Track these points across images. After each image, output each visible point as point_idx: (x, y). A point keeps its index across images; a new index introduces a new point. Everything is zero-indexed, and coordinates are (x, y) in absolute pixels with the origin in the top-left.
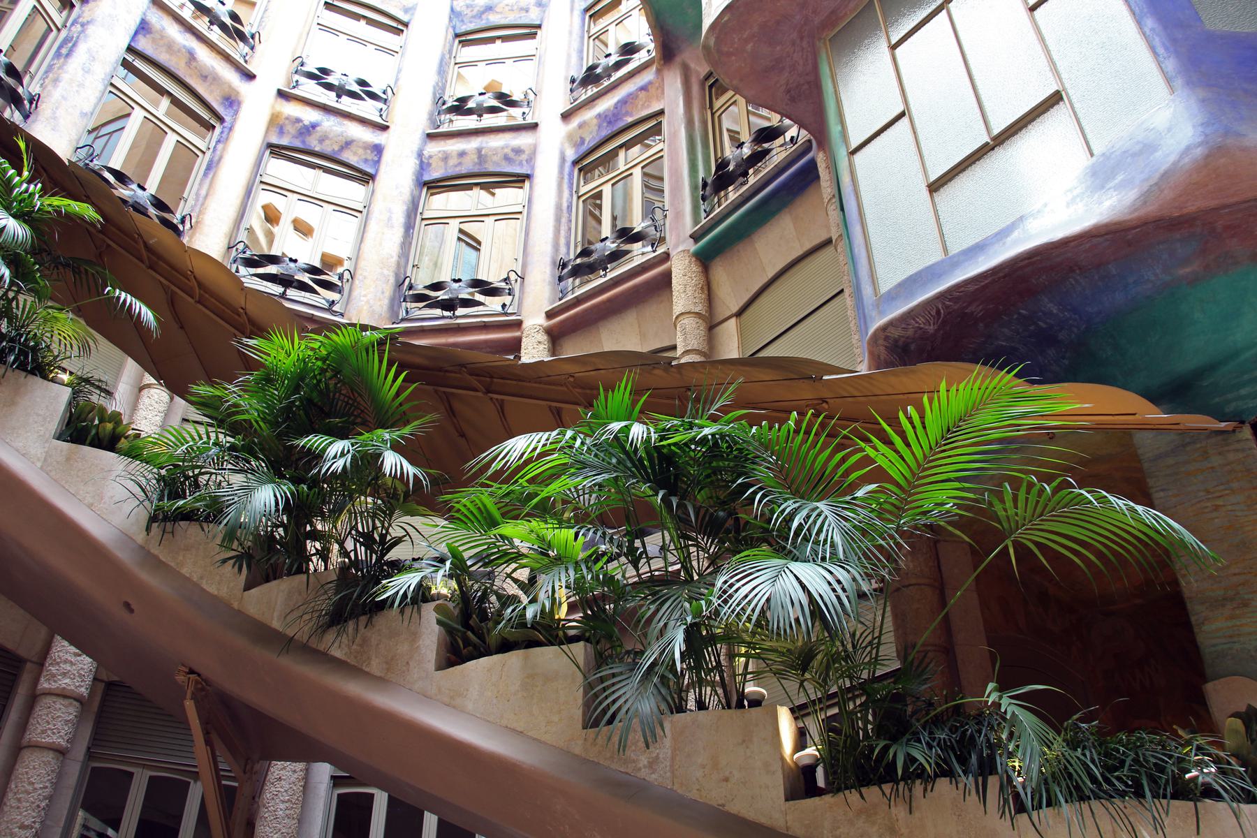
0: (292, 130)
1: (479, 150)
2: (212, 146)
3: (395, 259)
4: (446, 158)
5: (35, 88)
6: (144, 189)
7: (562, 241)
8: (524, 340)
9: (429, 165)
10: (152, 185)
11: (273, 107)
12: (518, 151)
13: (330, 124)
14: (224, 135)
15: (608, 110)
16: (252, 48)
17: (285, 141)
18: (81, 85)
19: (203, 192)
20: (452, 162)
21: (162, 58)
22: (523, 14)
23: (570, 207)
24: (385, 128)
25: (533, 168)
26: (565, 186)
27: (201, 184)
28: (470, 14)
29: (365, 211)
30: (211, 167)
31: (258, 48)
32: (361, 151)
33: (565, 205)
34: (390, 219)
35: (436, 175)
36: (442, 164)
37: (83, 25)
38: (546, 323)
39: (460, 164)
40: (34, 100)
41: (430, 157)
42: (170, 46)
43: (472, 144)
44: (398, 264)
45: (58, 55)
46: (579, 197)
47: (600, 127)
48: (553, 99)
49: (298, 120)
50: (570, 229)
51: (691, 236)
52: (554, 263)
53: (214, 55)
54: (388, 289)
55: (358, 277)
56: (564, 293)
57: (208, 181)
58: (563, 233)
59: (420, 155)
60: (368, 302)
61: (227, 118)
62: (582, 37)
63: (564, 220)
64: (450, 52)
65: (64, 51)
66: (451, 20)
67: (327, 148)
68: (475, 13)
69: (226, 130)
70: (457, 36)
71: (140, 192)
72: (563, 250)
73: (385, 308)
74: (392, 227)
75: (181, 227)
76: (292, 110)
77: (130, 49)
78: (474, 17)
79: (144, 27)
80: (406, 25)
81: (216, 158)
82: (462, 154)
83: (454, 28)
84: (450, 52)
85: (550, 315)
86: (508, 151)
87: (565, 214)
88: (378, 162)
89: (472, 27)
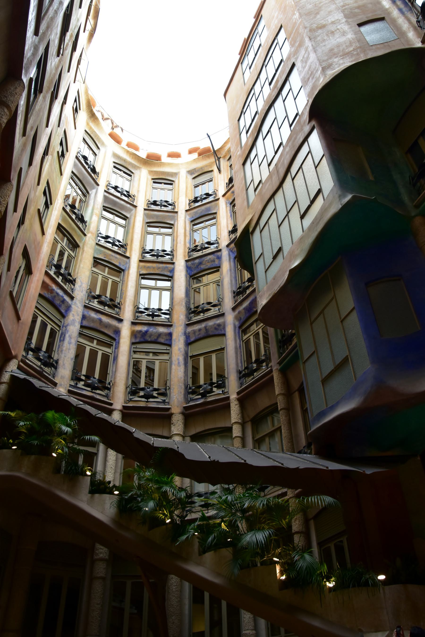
0: (139, 335)
1: (205, 327)
2: (113, 351)
3: (183, 379)
4: (194, 332)
5: (55, 358)
6: (95, 378)
7: (239, 361)
8: (231, 404)
9: (189, 336)
10: (97, 375)
11: (131, 329)
12: (219, 325)
13: (152, 330)
14: (117, 345)
15: (247, 306)
16: (120, 308)
17: (138, 340)
18: (69, 349)
19: (114, 370)
20: (197, 334)
21: (92, 325)
22: (213, 263)
23: (240, 346)
24: (171, 326)
25: (225, 331)
26: (237, 338)
27: (113, 367)
28: (194, 267)
29: (170, 360)
30: (116, 359)
31: (122, 307)
32: (164, 337)
33: (238, 346)
34: (179, 363)
35: (192, 339)
36: (194, 335)
37: (66, 327)
38: (237, 397)
39: (200, 334)
40: (57, 362)
41: (189, 333)
42: (93, 320)
43: (203, 325)
44: (185, 380)
45: (60, 341)
46: (243, 341)
47: (245, 313)
48: (228, 302)
49: (141, 331)
50: (241, 355)
51: (278, 363)
52: (237, 371)
53: (107, 317)
54: (183, 391)
55: (172, 388)
56: (241, 384)
57: (115, 365)
58: (239, 358)
59: (185, 333)
60: (176, 398)
61: (117, 338)
62: (235, 271)
63: (239, 353)
64: (189, 285)
65: (62, 339)
66: (187, 271)
67: (153, 338)
68: (195, 266)
69: (117, 343)
70: (191, 276)
71: (94, 380)
72: (240, 365)
73: (183, 398)
74: (180, 366)
75: (109, 386)
76: (138, 328)
77: (82, 327)
78: (195, 268)
79: (84, 317)
80: (172, 277)
81: (116, 355)
82: (200, 330)
83: (189, 274)
84: (189, 285)
85: (238, 393)
86: (215, 326)
87: (239, 350)
88: (171, 339)
89: (195, 272)
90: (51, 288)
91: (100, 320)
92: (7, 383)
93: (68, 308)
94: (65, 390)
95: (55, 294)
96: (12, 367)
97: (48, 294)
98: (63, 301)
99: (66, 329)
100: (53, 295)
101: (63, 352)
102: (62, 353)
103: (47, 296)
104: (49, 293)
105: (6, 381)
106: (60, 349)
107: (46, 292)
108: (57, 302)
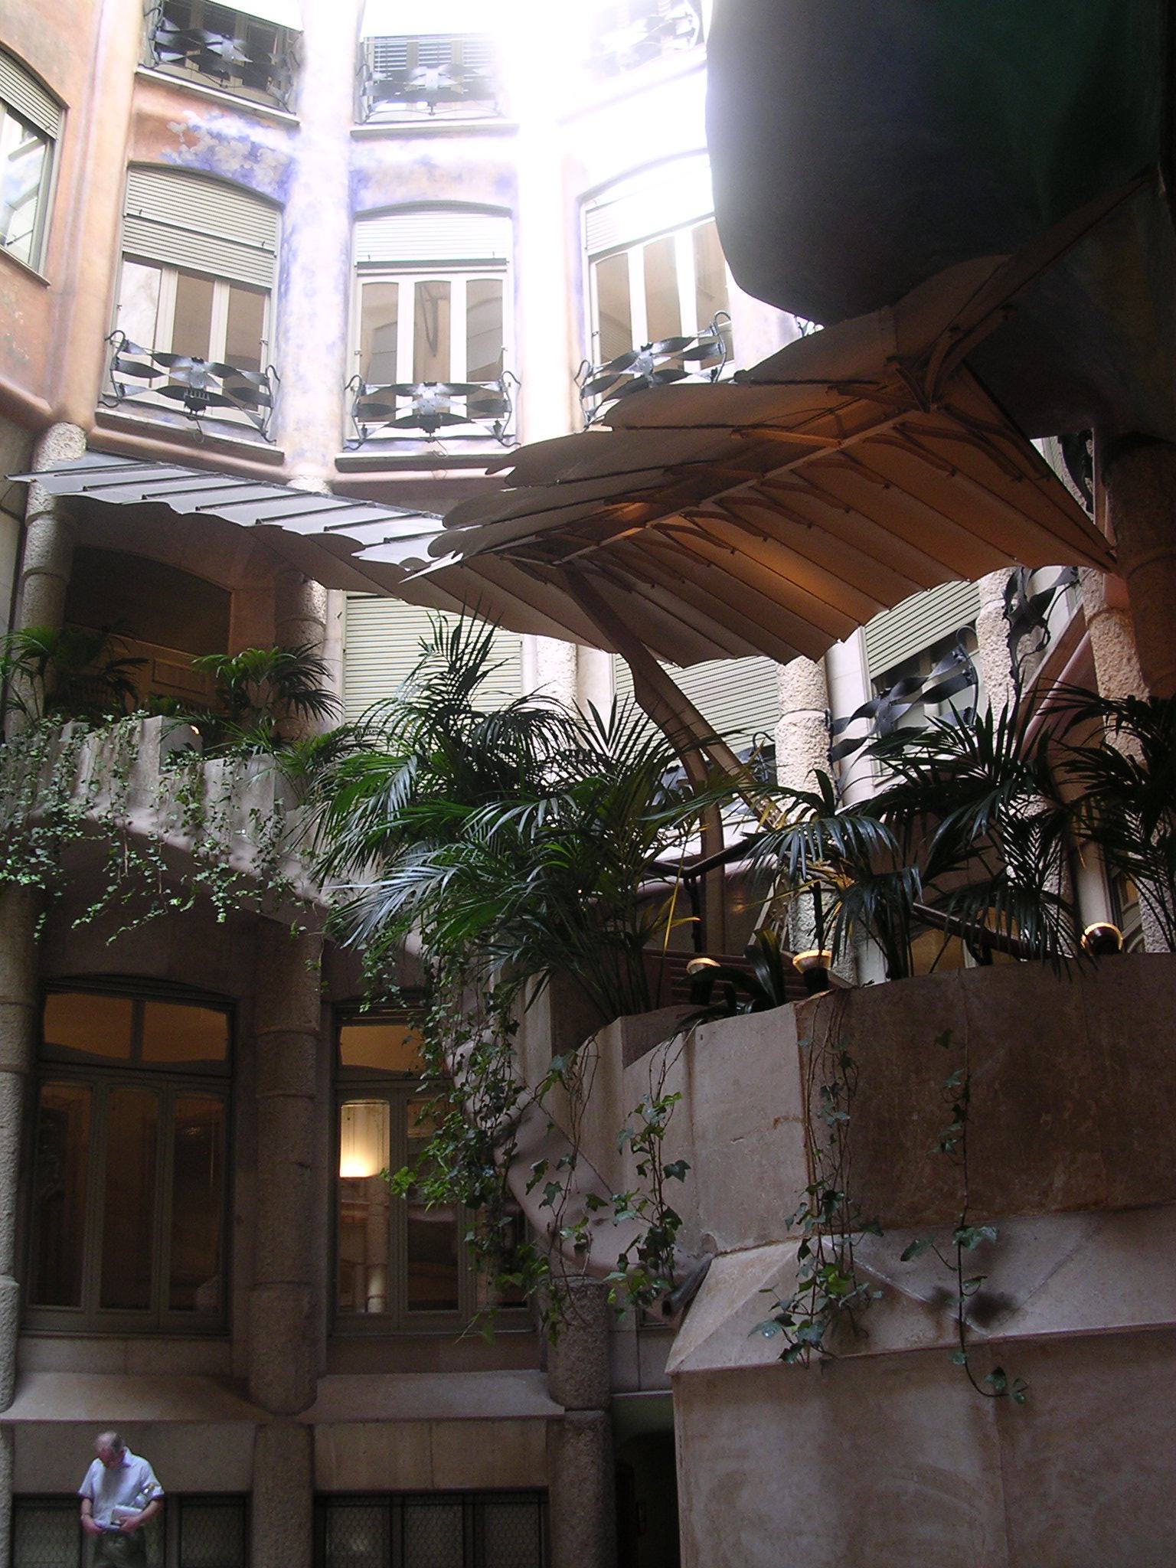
42: (400, 176)
79: (359, 179)
90: (182, 127)
91: (428, 166)
92: (48, 513)
93: (285, 173)
94: (325, 464)
95: (209, 141)
96: (63, 449)
97: (180, 153)
98: (254, 153)
99: (290, 250)
100: (201, 147)
101: (290, 334)
102: (287, 340)
103: (179, 162)
104: (184, 148)
105: (41, 509)
106: (282, 329)
107: (168, 150)
108: (230, 166)
